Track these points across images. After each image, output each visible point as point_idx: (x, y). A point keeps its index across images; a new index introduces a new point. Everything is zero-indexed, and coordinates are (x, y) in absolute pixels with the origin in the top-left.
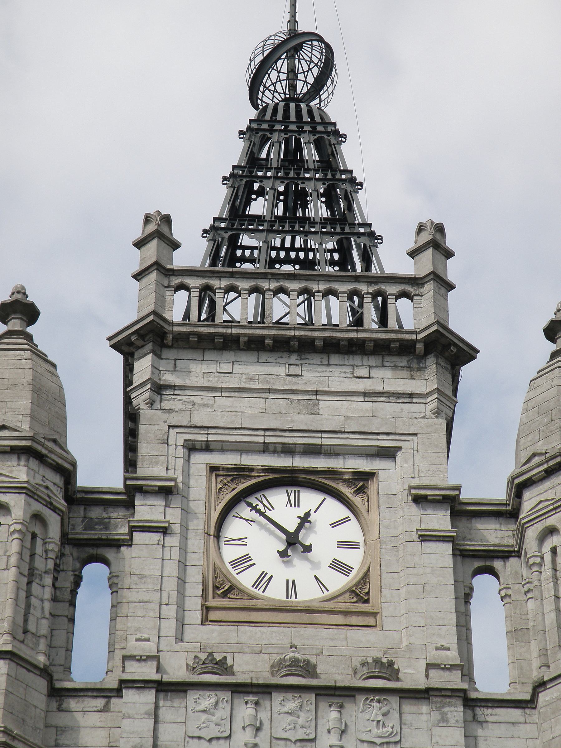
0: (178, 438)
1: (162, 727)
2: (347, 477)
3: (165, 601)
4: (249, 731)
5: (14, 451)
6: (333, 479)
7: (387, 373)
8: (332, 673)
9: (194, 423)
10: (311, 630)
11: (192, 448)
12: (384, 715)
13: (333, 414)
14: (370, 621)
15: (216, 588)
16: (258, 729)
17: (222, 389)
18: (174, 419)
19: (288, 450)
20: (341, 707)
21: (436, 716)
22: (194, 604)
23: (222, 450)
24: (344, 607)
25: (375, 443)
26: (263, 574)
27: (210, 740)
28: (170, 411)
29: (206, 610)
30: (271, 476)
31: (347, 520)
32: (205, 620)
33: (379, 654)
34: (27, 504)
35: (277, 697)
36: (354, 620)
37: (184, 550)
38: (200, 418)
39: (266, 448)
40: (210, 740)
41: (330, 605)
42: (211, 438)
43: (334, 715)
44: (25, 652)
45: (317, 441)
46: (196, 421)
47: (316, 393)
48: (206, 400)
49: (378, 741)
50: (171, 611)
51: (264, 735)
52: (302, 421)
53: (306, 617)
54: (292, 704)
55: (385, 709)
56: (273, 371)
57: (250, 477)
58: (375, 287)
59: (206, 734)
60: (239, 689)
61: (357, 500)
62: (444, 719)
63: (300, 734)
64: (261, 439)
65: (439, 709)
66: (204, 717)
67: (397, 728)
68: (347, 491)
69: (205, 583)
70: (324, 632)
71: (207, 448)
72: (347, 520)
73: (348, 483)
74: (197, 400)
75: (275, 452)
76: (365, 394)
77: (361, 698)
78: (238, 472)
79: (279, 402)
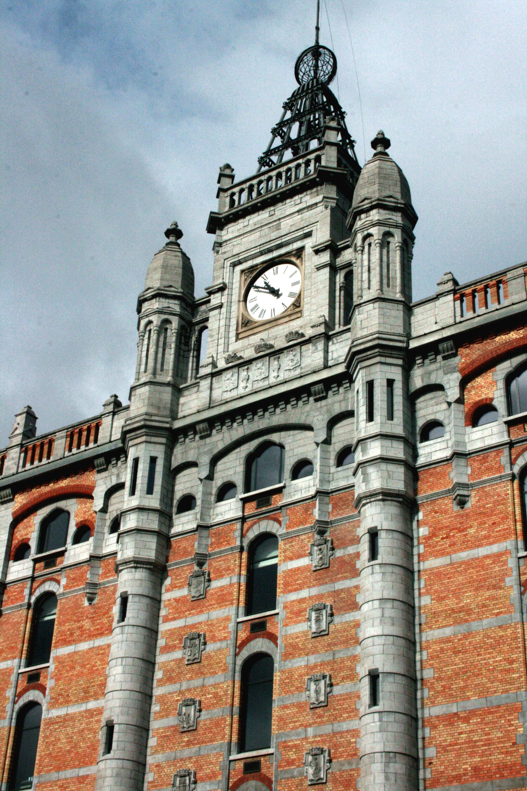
0: (228, 264)
1: (213, 392)
2: (294, 253)
3: (220, 337)
4: (245, 382)
5: (154, 297)
6: (289, 256)
7: (308, 197)
8: (280, 344)
9: (234, 254)
10: (276, 328)
11: (234, 265)
12: (294, 356)
13: (286, 226)
14: (299, 315)
15: (242, 323)
16: (248, 380)
17: (244, 234)
18: (226, 256)
19: (270, 250)
20: (279, 358)
21: (314, 348)
22: (233, 334)
23: (246, 261)
24: (289, 313)
25: (302, 233)
26: (263, 310)
27: (230, 391)
28: (225, 253)
29: (237, 334)
30: (265, 265)
31: (296, 272)
32: (237, 339)
33: (297, 329)
34: (159, 317)
35: (254, 363)
36: (293, 317)
37: (229, 312)
38: (236, 251)
39: (262, 253)
40: (230, 391)
41: (284, 315)
42: (240, 258)
43: (276, 363)
44: (160, 378)
45: (279, 242)
46: (234, 253)
47: (279, 219)
48: (239, 242)
49: (292, 368)
50: (221, 341)
51: (250, 381)
52: (274, 235)
53: (274, 323)
54: (259, 365)
55: (294, 353)
56: (263, 216)
57: (257, 269)
58: (305, 159)
59: (229, 389)
60: (239, 366)
61: (298, 262)
62: (316, 349)
63: (263, 376)
64: (258, 250)
65: (315, 345)
66: (228, 381)
67: (299, 360)
68: (293, 259)
69: (237, 324)
70: (281, 327)
71: (240, 263)
72: (296, 272)
73: (294, 255)
74: (235, 243)
75: (265, 253)
76: (298, 211)
77: (285, 351)
78: (252, 269)
79: (266, 229)
